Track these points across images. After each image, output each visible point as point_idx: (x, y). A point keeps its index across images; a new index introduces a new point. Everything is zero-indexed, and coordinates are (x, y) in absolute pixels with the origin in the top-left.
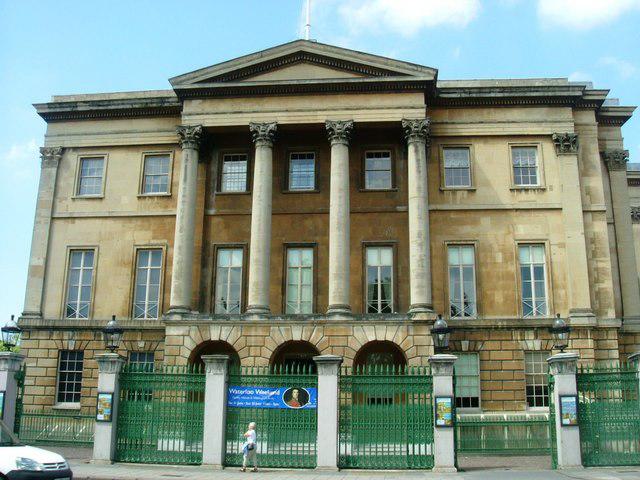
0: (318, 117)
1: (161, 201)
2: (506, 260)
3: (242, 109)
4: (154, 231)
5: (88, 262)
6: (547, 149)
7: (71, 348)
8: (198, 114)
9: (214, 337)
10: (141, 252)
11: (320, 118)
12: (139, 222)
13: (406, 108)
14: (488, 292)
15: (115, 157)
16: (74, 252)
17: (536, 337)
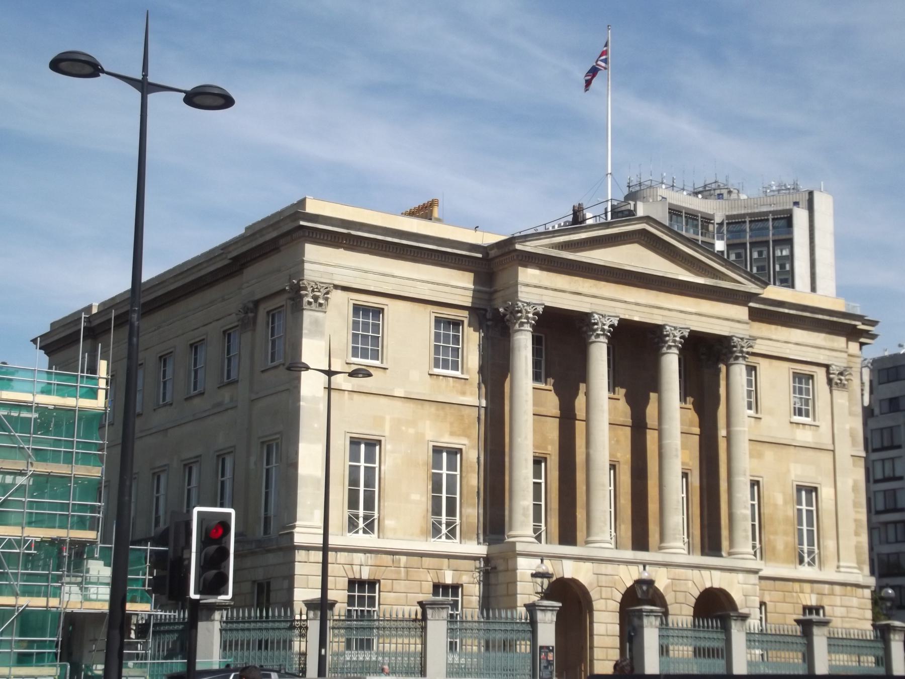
0: (655, 317)
1: (459, 384)
2: (785, 503)
3: (580, 290)
4: (451, 424)
5: (370, 458)
6: (820, 375)
7: (365, 576)
8: (535, 287)
9: (567, 575)
10: (437, 451)
11: (655, 318)
12: (432, 409)
13: (733, 320)
14: (772, 537)
15: (392, 309)
16: (355, 442)
17: (812, 592)
